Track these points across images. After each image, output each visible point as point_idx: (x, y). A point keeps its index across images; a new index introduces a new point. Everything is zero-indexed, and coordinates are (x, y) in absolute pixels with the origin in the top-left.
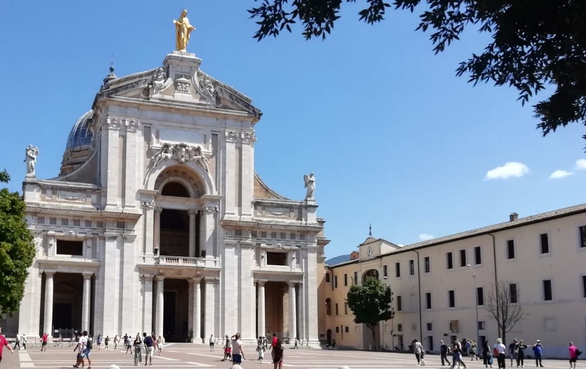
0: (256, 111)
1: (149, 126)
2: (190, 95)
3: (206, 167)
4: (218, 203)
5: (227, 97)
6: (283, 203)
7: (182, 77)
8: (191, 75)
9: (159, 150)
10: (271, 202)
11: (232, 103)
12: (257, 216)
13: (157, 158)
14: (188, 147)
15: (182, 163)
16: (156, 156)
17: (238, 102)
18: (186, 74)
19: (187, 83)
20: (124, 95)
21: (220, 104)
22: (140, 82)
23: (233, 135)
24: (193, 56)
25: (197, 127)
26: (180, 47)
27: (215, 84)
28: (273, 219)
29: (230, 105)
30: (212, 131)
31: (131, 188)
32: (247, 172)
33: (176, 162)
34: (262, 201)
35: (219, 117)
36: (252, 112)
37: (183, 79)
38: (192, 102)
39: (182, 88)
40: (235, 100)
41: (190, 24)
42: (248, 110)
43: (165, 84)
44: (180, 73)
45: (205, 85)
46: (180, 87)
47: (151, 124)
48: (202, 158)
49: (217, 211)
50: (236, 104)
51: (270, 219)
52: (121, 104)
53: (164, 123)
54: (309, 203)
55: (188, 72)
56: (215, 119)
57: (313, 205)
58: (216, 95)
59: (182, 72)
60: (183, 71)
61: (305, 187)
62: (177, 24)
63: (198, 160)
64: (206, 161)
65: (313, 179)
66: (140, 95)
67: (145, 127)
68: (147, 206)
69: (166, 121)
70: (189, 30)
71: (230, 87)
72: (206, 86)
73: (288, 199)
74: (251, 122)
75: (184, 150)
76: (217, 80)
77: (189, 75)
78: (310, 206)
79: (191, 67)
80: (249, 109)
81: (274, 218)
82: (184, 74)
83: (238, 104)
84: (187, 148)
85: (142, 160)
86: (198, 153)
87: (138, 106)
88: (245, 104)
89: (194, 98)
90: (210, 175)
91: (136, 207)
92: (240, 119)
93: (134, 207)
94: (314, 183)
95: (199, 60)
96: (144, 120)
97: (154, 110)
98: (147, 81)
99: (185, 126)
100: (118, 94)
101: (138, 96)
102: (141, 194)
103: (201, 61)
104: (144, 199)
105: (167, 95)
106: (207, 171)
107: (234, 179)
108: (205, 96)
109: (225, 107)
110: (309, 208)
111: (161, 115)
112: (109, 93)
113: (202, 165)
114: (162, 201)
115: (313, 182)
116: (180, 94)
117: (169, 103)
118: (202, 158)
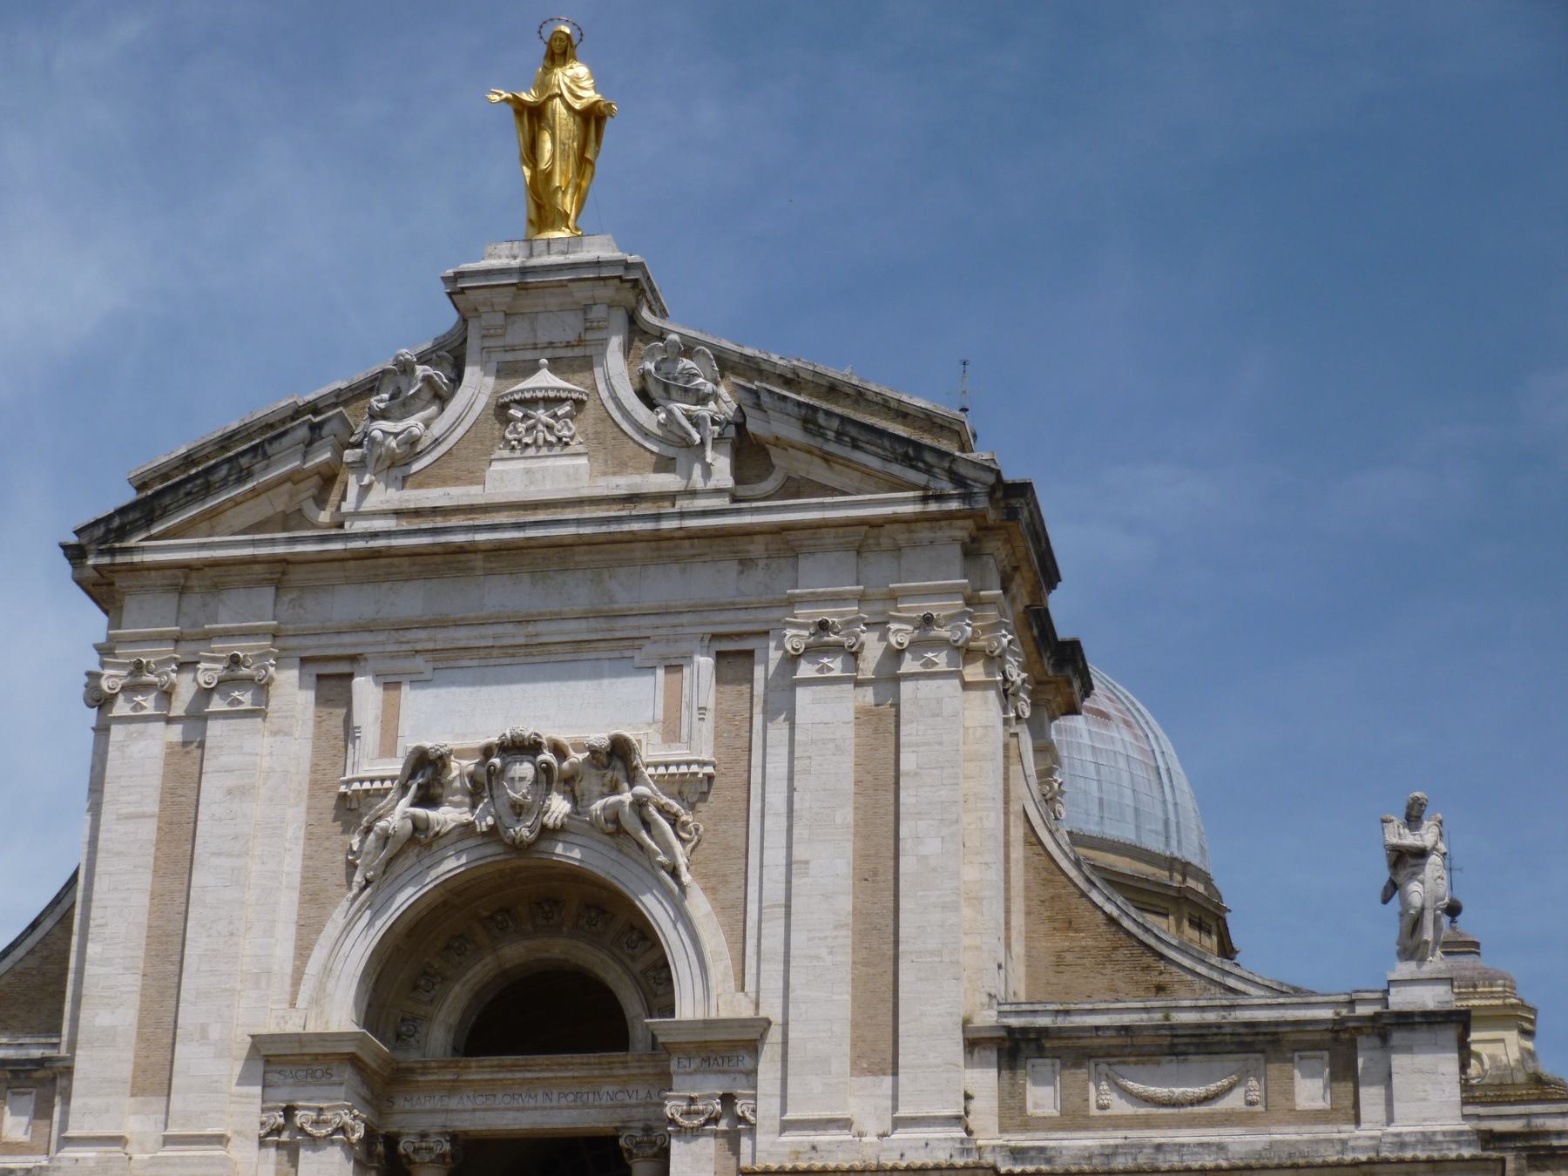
0: (963, 470)
1: (343, 668)
2: (583, 461)
3: (668, 850)
4: (747, 1063)
5: (792, 432)
6: (1211, 1017)
7: (533, 368)
8: (589, 352)
9: (387, 791)
10: (1126, 1019)
11: (827, 458)
12: (1027, 1124)
13: (372, 836)
14: (559, 751)
15: (518, 847)
16: (368, 830)
17: (855, 446)
18: (569, 353)
19: (560, 401)
20: (204, 526)
21: (761, 478)
22: (276, 446)
23: (833, 638)
24: (599, 249)
25: (625, 628)
26: (544, 213)
27: (726, 364)
28: (1135, 1135)
29: (820, 473)
30: (715, 637)
31: (204, 1029)
32: (932, 847)
33: (490, 850)
34: (1062, 1022)
35: (757, 548)
36: (947, 487)
37: (545, 380)
38: (586, 492)
39: (529, 430)
40: (839, 435)
41: (596, 89)
42: (921, 479)
43: (437, 429)
44: (529, 355)
45: (666, 387)
46: (521, 427)
47: (353, 659)
48: (639, 804)
49: (742, 1119)
50: (848, 463)
51: (1114, 1138)
52: (182, 578)
53: (423, 639)
54: (1402, 999)
55: (571, 337)
56: (732, 568)
57: (1431, 1005)
58: (731, 432)
59: (535, 347)
60: (543, 339)
61: (1385, 901)
62: (520, 107)
63: (615, 819)
64: (674, 820)
65: (1426, 836)
66: (300, 510)
67: (320, 677)
68: (301, 1130)
69: (441, 623)
70: (591, 119)
71: (820, 369)
72: (674, 393)
73: (1297, 991)
74: (957, 550)
75: (524, 769)
76: (748, 351)
77: (578, 352)
78: (1407, 1020)
79: (586, 309)
80: (929, 470)
81: (1147, 1123)
82: (549, 353)
83: (858, 456)
84: (547, 756)
85: (293, 864)
86: (620, 775)
87: (279, 573)
88: (900, 450)
89: (604, 474)
90: (699, 904)
91: (235, 1141)
92: (885, 542)
93: (220, 1140)
94: (1434, 859)
95: (628, 266)
96: (310, 641)
97: (373, 579)
98: (326, 430)
99: (549, 632)
100: (155, 530)
101: (290, 520)
102: (268, 1060)
103: (640, 266)
104: (282, 1095)
105: (444, 482)
106: (674, 873)
107: (845, 903)
108: (670, 452)
109: (794, 488)
110: (1397, 1037)
111: (410, 600)
112: (108, 531)
113: (641, 846)
114: (454, 1088)
115: (1421, 854)
116: (521, 465)
117: (440, 522)
118: (639, 804)
